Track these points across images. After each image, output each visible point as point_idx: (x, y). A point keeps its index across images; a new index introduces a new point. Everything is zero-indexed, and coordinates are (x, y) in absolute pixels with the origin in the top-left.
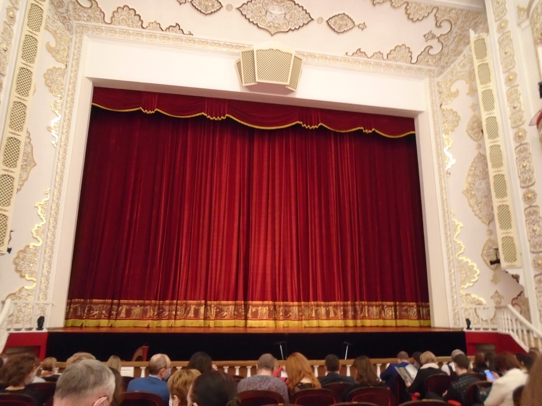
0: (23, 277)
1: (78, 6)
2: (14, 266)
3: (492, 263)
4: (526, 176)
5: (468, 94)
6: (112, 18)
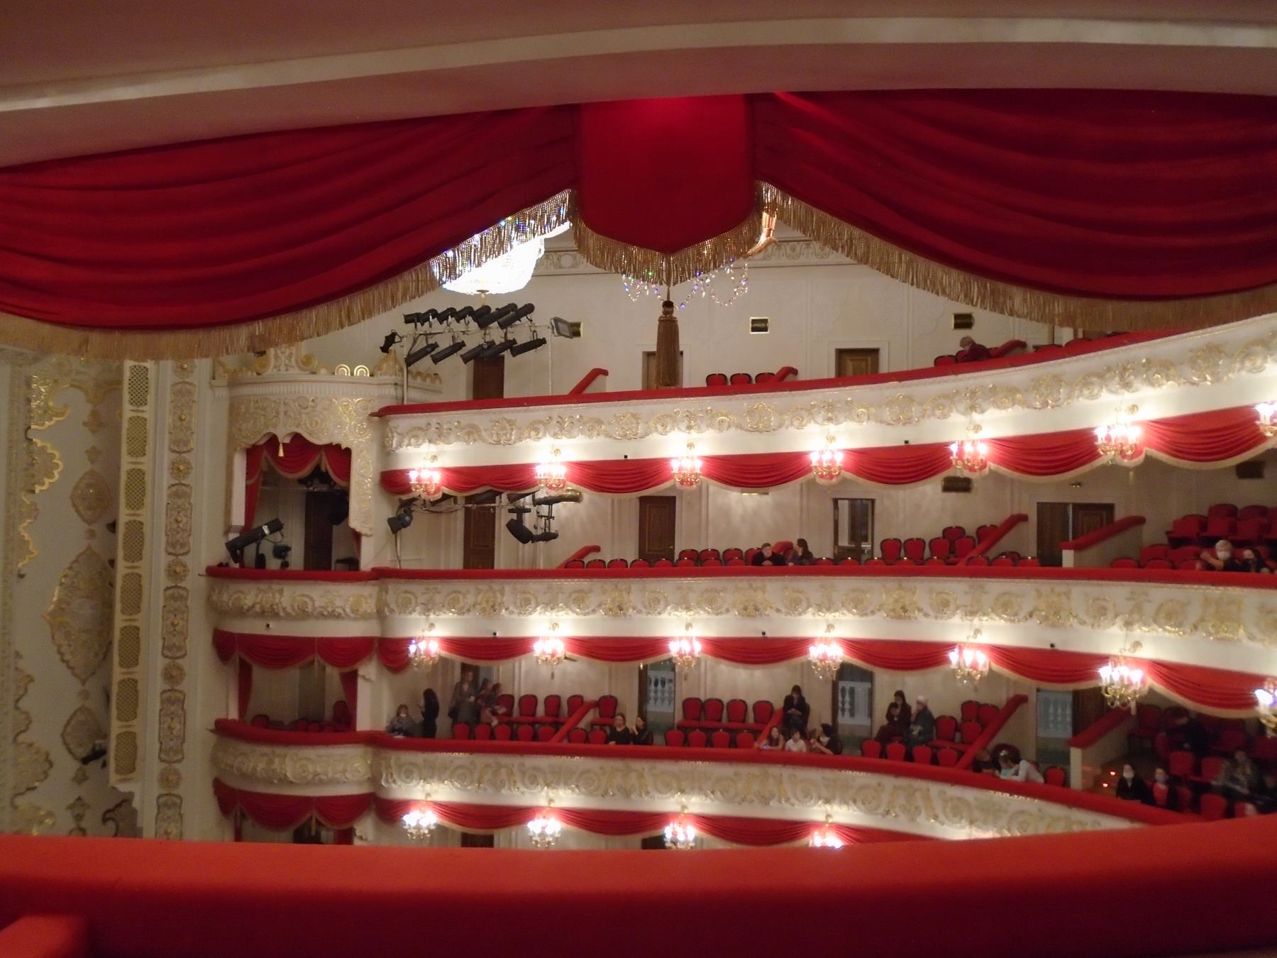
3: (85, 761)
4: (174, 640)
5: (85, 424)
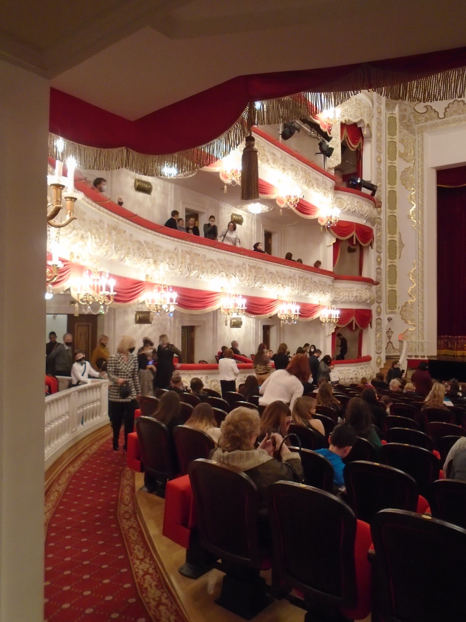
0: (406, 322)
1: (417, 114)
2: (400, 316)
6: (444, 113)
